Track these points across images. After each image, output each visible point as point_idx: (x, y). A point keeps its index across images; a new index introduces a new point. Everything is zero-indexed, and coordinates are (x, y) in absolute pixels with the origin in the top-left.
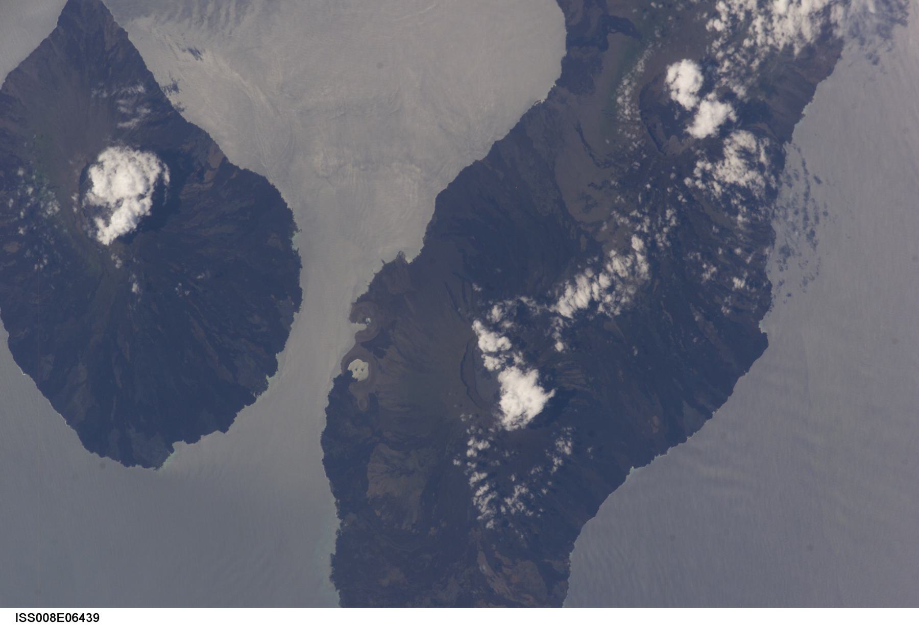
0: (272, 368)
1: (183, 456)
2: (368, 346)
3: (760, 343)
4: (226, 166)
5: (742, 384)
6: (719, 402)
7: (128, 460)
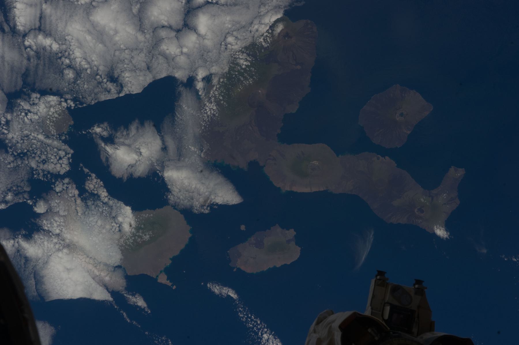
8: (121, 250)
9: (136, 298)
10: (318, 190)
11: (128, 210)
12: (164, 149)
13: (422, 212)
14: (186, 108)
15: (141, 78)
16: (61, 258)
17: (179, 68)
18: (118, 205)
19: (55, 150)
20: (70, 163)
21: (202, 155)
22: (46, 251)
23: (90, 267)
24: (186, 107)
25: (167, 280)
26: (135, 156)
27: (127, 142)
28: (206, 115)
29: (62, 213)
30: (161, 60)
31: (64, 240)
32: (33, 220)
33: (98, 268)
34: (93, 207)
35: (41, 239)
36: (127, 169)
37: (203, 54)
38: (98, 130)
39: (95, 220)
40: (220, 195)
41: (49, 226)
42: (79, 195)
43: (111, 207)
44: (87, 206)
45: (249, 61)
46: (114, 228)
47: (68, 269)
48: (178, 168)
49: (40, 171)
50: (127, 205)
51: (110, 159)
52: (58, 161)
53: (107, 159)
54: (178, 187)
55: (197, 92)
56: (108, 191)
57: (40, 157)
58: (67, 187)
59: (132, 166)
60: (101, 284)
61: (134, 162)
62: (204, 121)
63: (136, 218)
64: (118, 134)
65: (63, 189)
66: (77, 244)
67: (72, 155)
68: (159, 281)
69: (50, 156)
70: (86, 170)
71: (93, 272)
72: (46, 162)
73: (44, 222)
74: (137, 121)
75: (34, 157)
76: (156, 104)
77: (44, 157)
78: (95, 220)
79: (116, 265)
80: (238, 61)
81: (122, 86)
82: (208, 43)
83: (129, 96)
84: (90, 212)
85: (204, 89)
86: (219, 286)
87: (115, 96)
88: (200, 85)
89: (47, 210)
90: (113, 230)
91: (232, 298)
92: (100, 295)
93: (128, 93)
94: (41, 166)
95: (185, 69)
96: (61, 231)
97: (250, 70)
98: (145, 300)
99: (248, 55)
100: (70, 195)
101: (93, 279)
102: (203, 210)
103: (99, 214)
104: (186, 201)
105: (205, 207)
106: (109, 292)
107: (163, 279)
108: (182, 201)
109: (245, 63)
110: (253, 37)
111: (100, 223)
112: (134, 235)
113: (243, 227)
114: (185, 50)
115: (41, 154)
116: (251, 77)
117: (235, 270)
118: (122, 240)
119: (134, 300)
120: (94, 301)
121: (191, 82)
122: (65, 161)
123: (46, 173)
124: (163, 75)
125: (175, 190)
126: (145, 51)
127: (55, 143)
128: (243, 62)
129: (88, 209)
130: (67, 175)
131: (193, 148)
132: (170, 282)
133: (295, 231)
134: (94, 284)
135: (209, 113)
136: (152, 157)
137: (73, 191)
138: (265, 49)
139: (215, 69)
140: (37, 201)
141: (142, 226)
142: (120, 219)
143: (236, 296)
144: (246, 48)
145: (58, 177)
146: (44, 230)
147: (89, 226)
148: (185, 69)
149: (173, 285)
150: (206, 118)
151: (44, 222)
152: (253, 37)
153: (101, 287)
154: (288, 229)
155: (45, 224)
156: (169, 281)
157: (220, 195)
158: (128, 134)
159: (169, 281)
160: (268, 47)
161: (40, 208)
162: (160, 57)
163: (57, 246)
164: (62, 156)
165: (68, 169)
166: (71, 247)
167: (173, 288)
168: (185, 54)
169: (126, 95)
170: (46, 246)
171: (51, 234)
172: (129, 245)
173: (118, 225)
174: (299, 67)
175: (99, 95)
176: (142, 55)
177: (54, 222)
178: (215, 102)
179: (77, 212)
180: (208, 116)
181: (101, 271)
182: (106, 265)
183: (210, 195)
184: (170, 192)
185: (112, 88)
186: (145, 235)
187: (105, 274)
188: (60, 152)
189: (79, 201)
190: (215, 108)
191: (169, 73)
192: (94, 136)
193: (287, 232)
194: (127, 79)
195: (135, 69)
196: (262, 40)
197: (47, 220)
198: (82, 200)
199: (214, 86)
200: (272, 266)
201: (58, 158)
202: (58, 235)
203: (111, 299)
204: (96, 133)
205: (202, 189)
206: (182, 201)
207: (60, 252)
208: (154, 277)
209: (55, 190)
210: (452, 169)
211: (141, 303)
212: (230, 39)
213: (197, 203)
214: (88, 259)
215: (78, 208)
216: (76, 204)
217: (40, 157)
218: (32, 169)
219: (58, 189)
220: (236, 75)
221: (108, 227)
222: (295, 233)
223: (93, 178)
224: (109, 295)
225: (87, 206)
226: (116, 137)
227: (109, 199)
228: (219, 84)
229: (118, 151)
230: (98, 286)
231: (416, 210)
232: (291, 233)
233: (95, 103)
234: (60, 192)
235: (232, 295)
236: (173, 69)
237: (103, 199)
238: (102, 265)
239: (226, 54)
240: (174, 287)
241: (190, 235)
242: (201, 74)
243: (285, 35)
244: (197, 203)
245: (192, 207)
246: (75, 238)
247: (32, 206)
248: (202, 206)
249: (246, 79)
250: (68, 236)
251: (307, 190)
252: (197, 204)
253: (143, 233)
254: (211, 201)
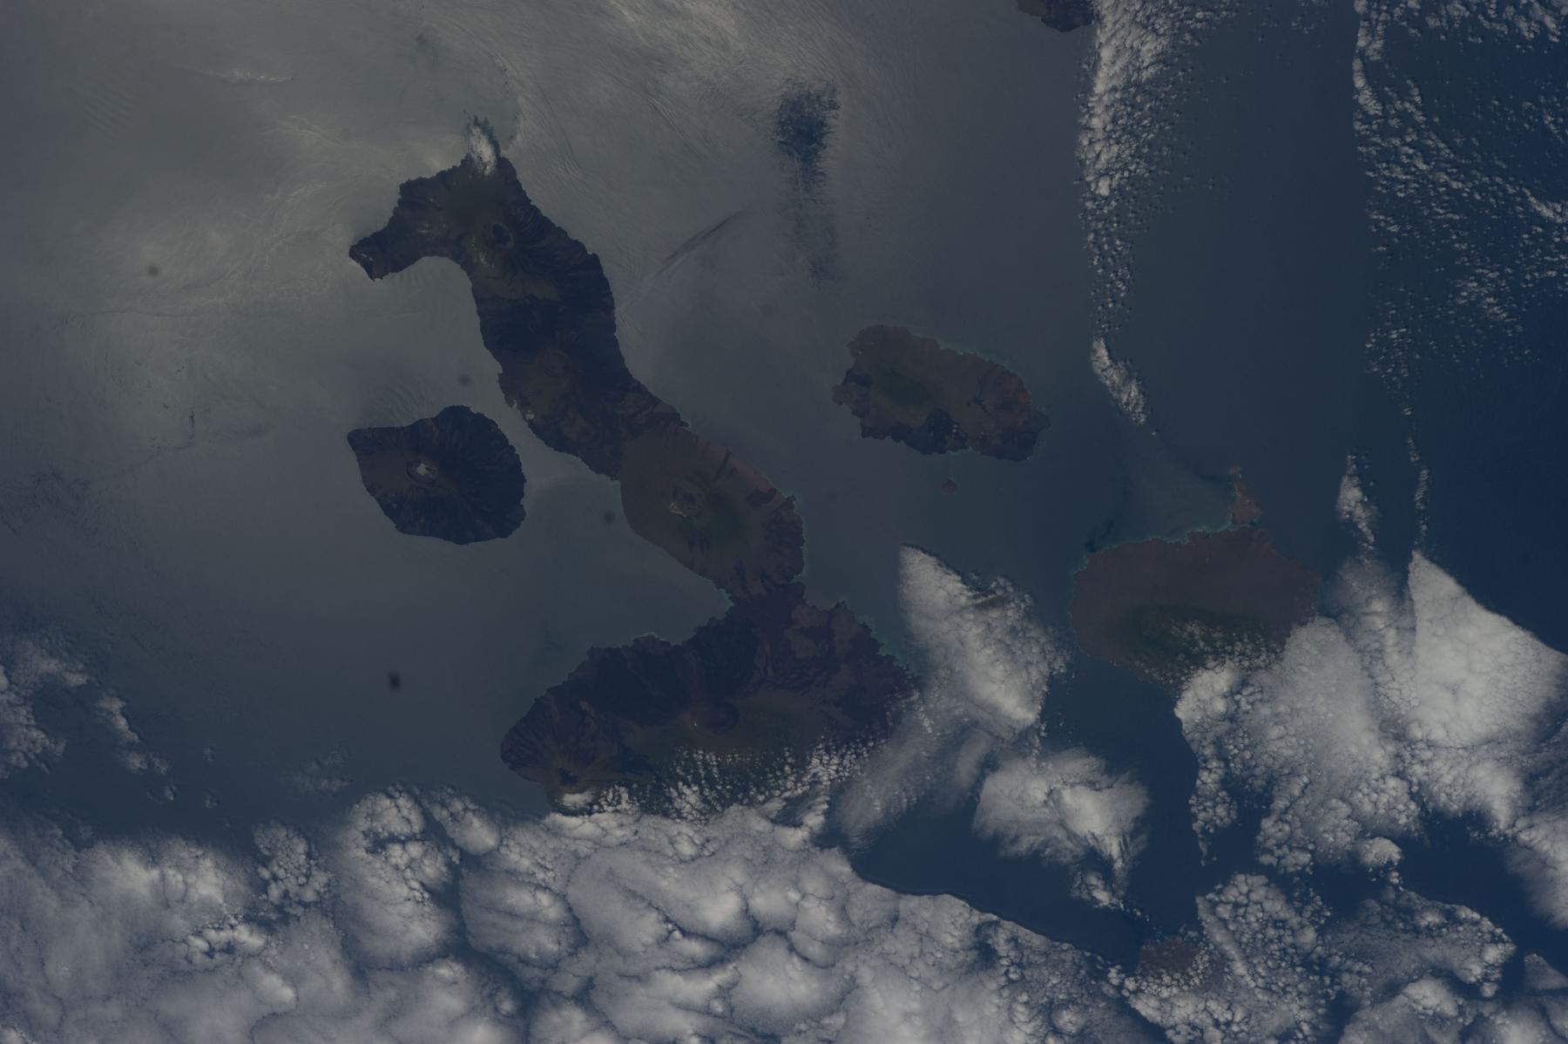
0: (513, 448)
1: (527, 503)
2: (524, 405)
3: (595, 257)
4: (435, 420)
5: (606, 273)
6: (608, 286)
7: (517, 524)
8: (1283, 644)
9: (1350, 513)
11: (1185, 710)
12: (989, 765)
14: (877, 803)
15: (926, 915)
16: (1444, 725)
17: (831, 878)
18: (1197, 736)
19: (1232, 927)
20: (1226, 881)
21: (916, 696)
22: (1466, 764)
23: (1393, 659)
24: (874, 802)
26: (1068, 797)
27: (1060, 834)
28: (845, 762)
29: (1344, 809)
30: (856, 914)
31: (1398, 756)
32: (1428, 842)
33: (1377, 645)
34: (1258, 771)
35: (1449, 795)
36: (1109, 787)
37: (765, 863)
38: (1103, 897)
39: (1280, 744)
40: (942, 593)
41: (1401, 807)
42: (1268, 813)
43: (1218, 743)
44: (1272, 780)
45: (677, 789)
46: (1251, 699)
47: (1454, 692)
48: (994, 710)
49: (1308, 914)
50: (1179, 720)
51: (1129, 826)
52: (1246, 906)
53: (1134, 834)
54: (1024, 674)
55: (826, 813)
56: (1197, 777)
57: (1280, 938)
58: (1279, 846)
59: (1092, 785)
60: (1407, 603)
61: (1078, 788)
62: (858, 755)
63: (1182, 683)
64: (1068, 859)
65: (1291, 849)
66: (1376, 728)
67: (1204, 895)
69: (1256, 926)
70: (1203, 847)
71: (1396, 645)
72: (1275, 922)
73: (1403, 820)
74: (1002, 853)
75: (1293, 946)
76: (933, 850)
77: (1271, 932)
78: (1282, 744)
79: (1325, 621)
80: (700, 805)
81: (978, 930)
82: (737, 874)
83: (976, 903)
84: (1276, 767)
85: (810, 808)
86: (1117, 401)
87: (1008, 925)
88: (814, 820)
89: (1372, 837)
90: (1259, 696)
91: (1108, 349)
92: (1433, 585)
93: (976, 912)
94: (1294, 921)
95: (821, 867)
96: (1383, 777)
97: (687, 772)
98: (1337, 493)
99: (670, 800)
100: (1287, 828)
101: (1413, 629)
102: (1011, 589)
103: (1259, 749)
104: (1033, 634)
105: (1000, 593)
106: (1406, 574)
108: (1043, 640)
109: (688, 792)
110: (637, 821)
111: (1275, 732)
112: (1220, 656)
114: (794, 896)
115: (1271, 941)
116: (694, 761)
118: (1258, 662)
119: (1359, 511)
120: (1460, 581)
121: (827, 839)
122: (1232, 894)
123: (1297, 904)
124: (873, 889)
125: (1037, 673)
126: (878, 950)
127: (1219, 937)
128: (690, 797)
129: (1276, 775)
130: (1253, 868)
131: (926, 723)
134: (1424, 615)
135: (835, 761)
136: (1031, 769)
137: (1272, 830)
138: (628, 786)
139: (760, 825)
140: (1377, 869)
141: (1180, 657)
142: (1220, 706)
143: (1095, 345)
144: (666, 815)
145: (1280, 880)
146: (1423, 806)
147: (1307, 742)
148: (821, 867)
150: (850, 757)
151: (1403, 820)
152: (637, 821)
153: (1416, 597)
155: (1406, 815)
157: (942, 593)
158: (1045, 844)
160: (620, 785)
161: (1384, 851)
162: (854, 919)
163: (1428, 754)
164: (1229, 907)
165: (1241, 878)
166: (1394, 729)
168: (798, 890)
169: (983, 910)
170: (1454, 773)
171: (1415, 789)
172: (1252, 641)
173: (1237, 697)
174: (585, 706)
175: (1042, 949)
176: (887, 947)
177: (1380, 805)
178: (806, 772)
179: (1306, 785)
180: (842, 757)
181: (1375, 633)
182: (1350, 637)
183: (961, 611)
184: (1051, 677)
185: (1002, 942)
186: (1192, 635)
187: (1374, 618)
188: (1226, 916)
189: (1280, 804)
190: (815, 761)
191: (861, 884)
192: (1121, 893)
194: (956, 933)
195: (925, 937)
196: (624, 805)
197: (1395, 821)
198: (1271, 800)
199: (786, 799)
201: (1242, 911)
202: (1400, 775)
203: (1417, 556)
204: (1114, 893)
205: (972, 631)
206: (1043, 640)
207: (1433, 737)
209: (1313, 859)
211: (1351, 496)
212: (687, 849)
213: (1010, 613)
214: (1380, 679)
215: (1297, 792)
216: (1292, 803)
217: (1280, 938)
218: (1321, 932)
219: (1305, 858)
220: (724, 786)
221: (1265, 711)
223: (1200, 823)
224: (1411, 566)
225: (1268, 783)
226: (1075, 857)
227: (1205, 761)
228: (772, 796)
229: (1097, 832)
230: (1417, 606)
231: (510, 244)
233: (1062, 942)
234: (1304, 849)
235: (1103, 352)
236: (844, 884)
237: (1220, 772)
238: (1362, 643)
239: (710, 831)
242: (794, 837)
243: (571, 782)
244: (1010, 613)
245: (1028, 615)
246: (1365, 741)
247: (1397, 870)
248: (999, 603)
249: (706, 764)
250: (1380, 757)
252: (1012, 614)
253: (1194, 644)
254: (975, 597)
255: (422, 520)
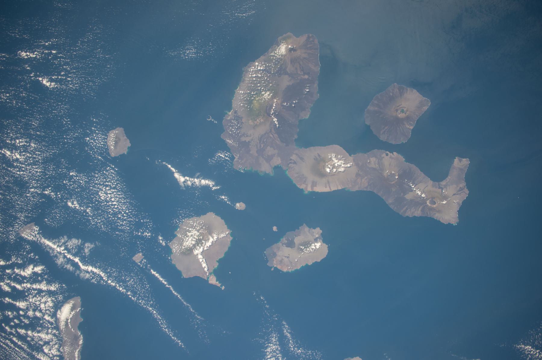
10: (336, 189)
13: (435, 203)
25: (217, 281)
68: (210, 282)
107: (213, 281)
113: (275, 229)
117: (272, 269)
132: (219, 283)
133: (321, 229)
149: (221, 286)
154: (314, 228)
156: (218, 283)
159: (218, 283)
167: (223, 289)
174: (306, 77)
193: (313, 230)
200: (304, 265)
208: (206, 278)
210: (456, 160)
222: (321, 231)
232: (317, 232)
240: (223, 288)
241: (231, 238)
251: (327, 190)
255: (391, 94)
